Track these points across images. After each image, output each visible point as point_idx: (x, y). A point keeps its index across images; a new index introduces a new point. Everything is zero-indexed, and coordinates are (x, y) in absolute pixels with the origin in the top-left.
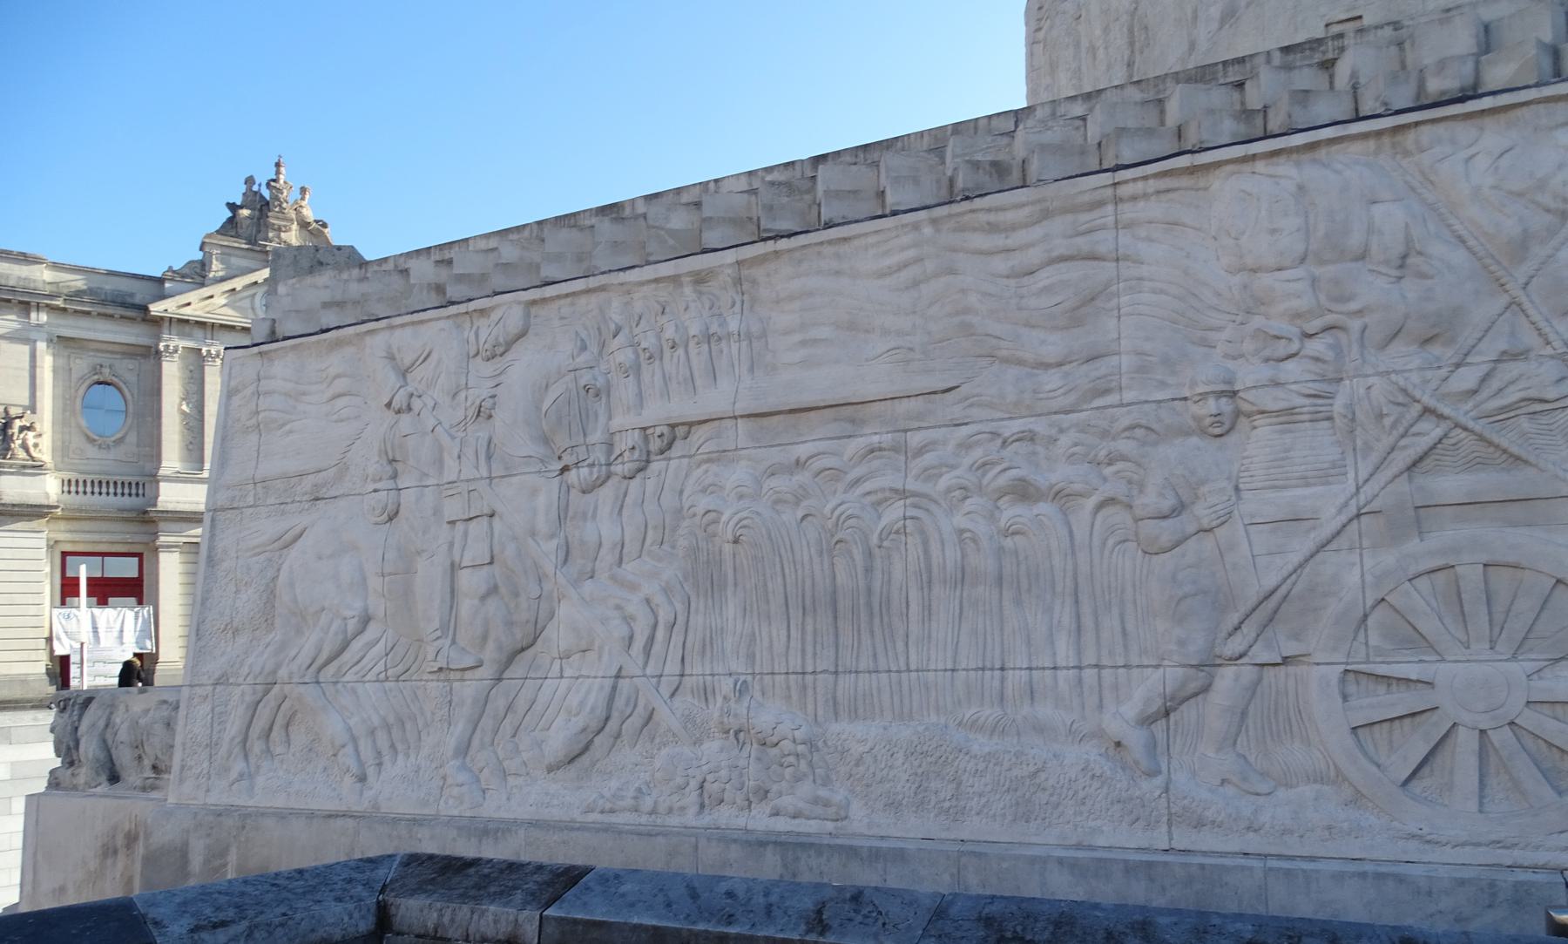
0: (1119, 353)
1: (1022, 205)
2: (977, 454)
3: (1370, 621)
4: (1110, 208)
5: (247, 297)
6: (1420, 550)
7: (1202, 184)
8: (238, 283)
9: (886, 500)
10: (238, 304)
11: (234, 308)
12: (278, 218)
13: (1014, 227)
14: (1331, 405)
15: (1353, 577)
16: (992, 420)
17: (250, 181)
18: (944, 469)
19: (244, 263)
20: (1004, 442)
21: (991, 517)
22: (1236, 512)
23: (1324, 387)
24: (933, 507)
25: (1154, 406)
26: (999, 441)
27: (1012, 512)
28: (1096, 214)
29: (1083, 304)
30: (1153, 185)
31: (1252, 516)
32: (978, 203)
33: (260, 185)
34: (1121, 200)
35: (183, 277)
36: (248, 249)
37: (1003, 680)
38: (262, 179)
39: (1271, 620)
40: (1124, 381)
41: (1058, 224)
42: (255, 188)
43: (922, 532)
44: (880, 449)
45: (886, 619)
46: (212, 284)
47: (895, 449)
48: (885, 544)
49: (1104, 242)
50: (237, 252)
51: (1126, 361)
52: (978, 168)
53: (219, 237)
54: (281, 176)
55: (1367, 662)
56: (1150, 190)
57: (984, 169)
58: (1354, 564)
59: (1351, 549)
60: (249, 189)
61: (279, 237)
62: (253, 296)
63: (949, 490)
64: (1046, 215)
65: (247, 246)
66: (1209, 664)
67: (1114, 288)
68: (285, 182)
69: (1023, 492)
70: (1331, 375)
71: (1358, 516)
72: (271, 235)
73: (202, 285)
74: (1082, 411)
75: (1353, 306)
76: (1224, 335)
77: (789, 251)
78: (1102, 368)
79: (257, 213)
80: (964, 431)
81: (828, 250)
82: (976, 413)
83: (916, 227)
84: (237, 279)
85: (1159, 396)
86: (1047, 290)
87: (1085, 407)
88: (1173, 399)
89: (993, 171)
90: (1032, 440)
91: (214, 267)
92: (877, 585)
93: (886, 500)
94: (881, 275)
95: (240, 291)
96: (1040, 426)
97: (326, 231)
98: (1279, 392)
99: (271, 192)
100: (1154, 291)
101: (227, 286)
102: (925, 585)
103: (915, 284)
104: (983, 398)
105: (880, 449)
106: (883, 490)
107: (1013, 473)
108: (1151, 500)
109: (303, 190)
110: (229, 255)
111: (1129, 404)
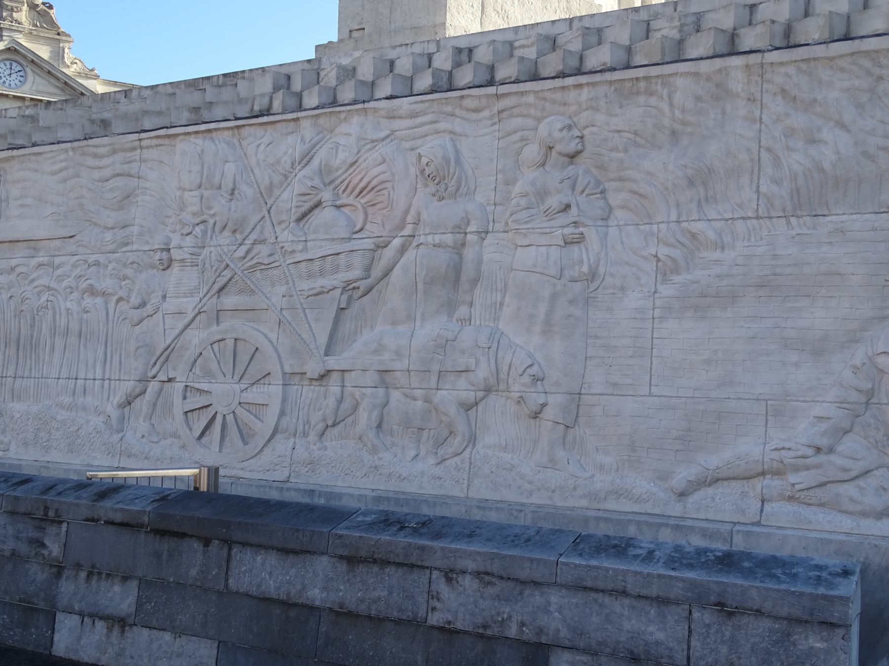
0: (134, 225)
1: (104, 146)
2: (78, 271)
3: (197, 363)
4: (139, 151)
6: (215, 331)
7: (173, 143)
9: (43, 291)
13: (102, 157)
14: (198, 259)
15: (196, 341)
16: (86, 254)
18: (65, 277)
20: (89, 265)
21: (79, 303)
22: (161, 307)
23: (197, 250)
24: (59, 297)
25: (142, 253)
26: (87, 265)
27: (88, 301)
28: (133, 153)
29: (124, 199)
30: (155, 142)
31: (166, 310)
32: (90, 142)
34: (143, 148)
37: (76, 383)
39: (167, 361)
40: (134, 240)
41: (119, 157)
43: (54, 308)
44: (43, 265)
45: (37, 351)
47: (48, 265)
48: (40, 313)
49: (134, 168)
51: (135, 229)
52: (94, 123)
55: (193, 382)
56: (153, 144)
57: (97, 124)
58: (196, 336)
59: (197, 328)
61: (11, 16)
63: (65, 288)
64: (114, 152)
66: (144, 380)
67: (137, 192)
69: (92, 291)
70: (200, 245)
71: (200, 313)
72: (4, 14)
74: (118, 253)
75: (212, 212)
76: (171, 220)
77: (18, 156)
78: (127, 231)
80: (76, 258)
81: (33, 158)
82: (81, 250)
83: (66, 151)
85: (146, 248)
86: (111, 190)
87: (119, 251)
88: (150, 250)
89: (101, 125)
90: (99, 265)
92: (35, 334)
93: (43, 291)
94: (53, 174)
96: (102, 258)
97: (51, 12)
98: (180, 251)
100: (151, 195)
102: (53, 335)
103: (65, 180)
104: (84, 242)
105: (43, 265)
106: (41, 285)
107: (89, 281)
108: (135, 300)
111: (134, 251)
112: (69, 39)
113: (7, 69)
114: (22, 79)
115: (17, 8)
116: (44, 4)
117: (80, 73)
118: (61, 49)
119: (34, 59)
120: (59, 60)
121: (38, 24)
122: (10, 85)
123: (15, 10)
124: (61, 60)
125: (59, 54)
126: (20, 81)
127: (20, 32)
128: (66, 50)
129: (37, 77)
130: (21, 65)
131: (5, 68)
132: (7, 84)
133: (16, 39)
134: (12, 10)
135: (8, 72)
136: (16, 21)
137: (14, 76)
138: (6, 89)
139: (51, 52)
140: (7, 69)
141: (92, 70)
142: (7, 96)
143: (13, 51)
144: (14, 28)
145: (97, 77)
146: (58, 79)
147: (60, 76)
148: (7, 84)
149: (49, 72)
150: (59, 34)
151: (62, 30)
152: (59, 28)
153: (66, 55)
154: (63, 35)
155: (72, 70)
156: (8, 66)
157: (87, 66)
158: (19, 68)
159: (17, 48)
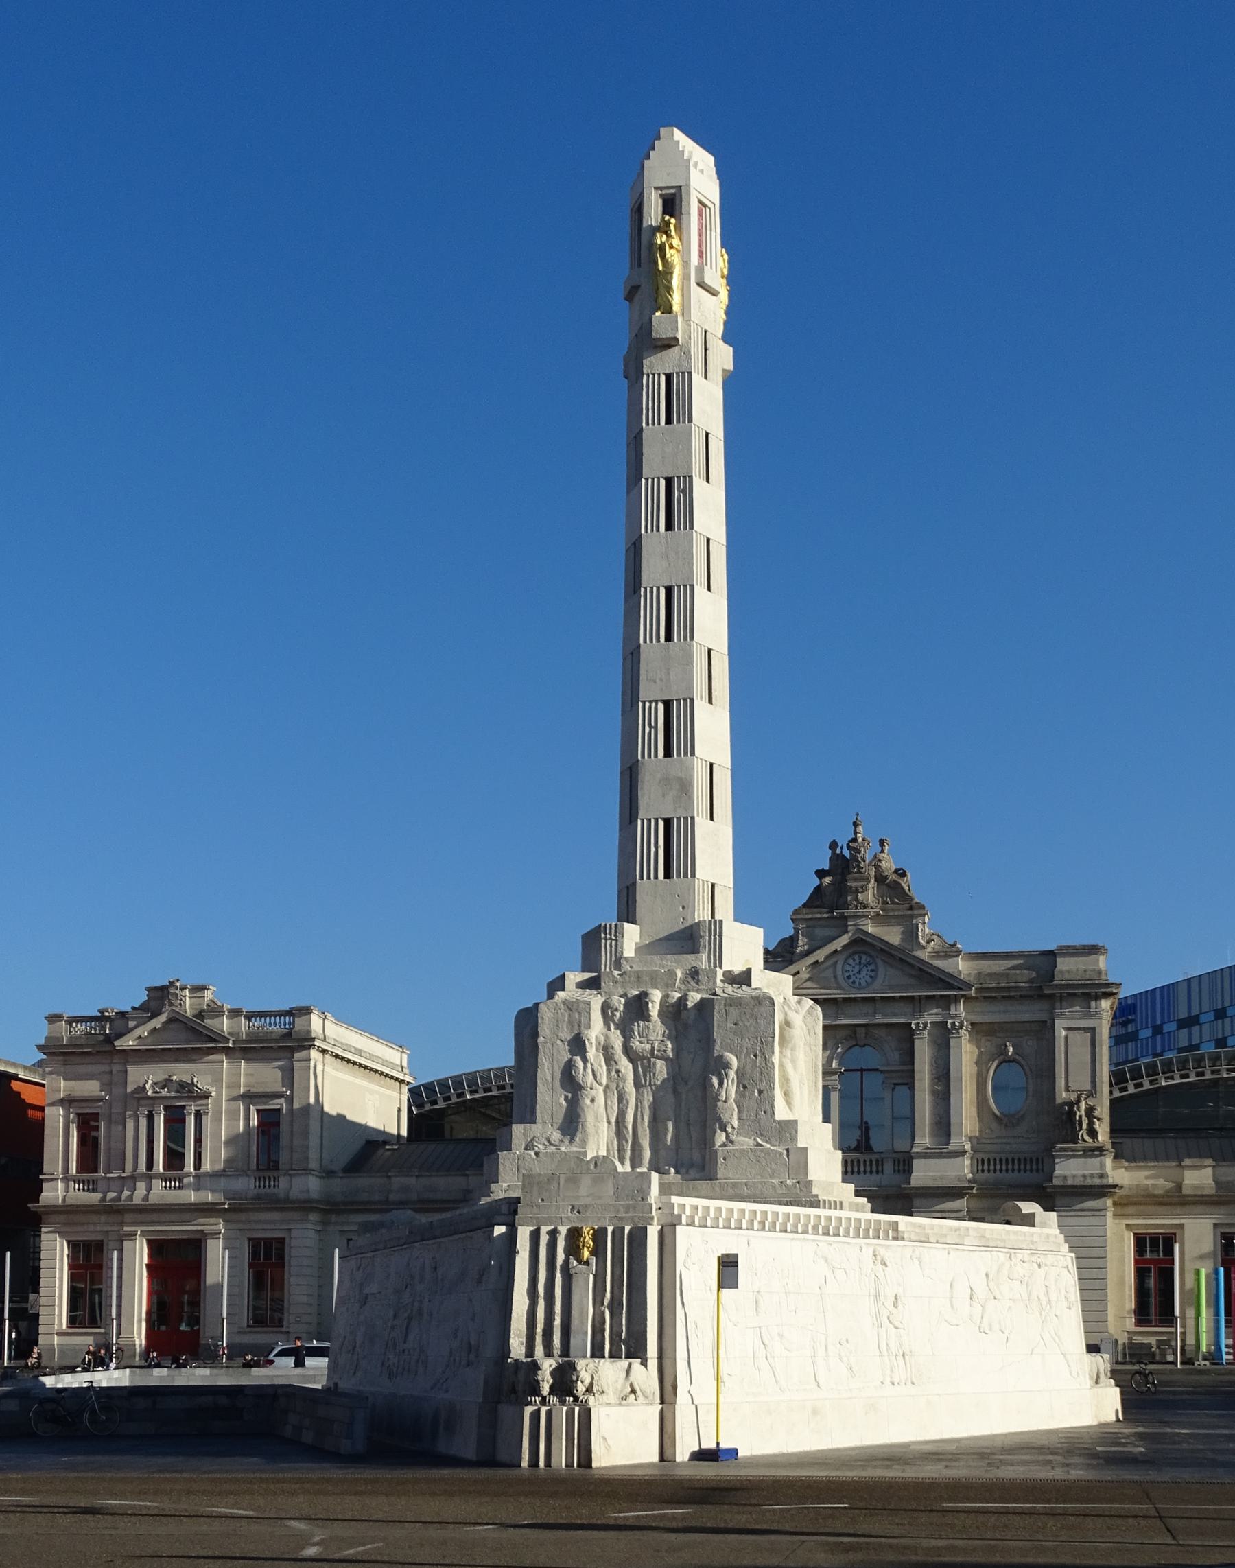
5: (829, 966)
8: (820, 955)
10: (823, 975)
11: (817, 983)
17: (834, 845)
19: (827, 932)
33: (842, 848)
35: (777, 957)
38: (843, 841)
42: (838, 851)
50: (821, 922)
53: (808, 910)
54: (859, 835)
60: (834, 853)
61: (857, 899)
68: (863, 840)
73: (791, 962)
84: (818, 952)
91: (800, 943)
95: (823, 962)
99: (851, 853)
101: (810, 960)
109: (882, 843)
110: (814, 927)
112: (922, 912)
113: (856, 964)
114: (872, 974)
117: (938, 952)
119: (882, 947)
122: (860, 984)
124: (915, 941)
125: (911, 934)
126: (871, 977)
127: (867, 917)
128: (920, 926)
130: (871, 956)
131: (853, 964)
132: (857, 983)
133: (861, 927)
135: (857, 969)
136: (861, 904)
137: (864, 972)
138: (854, 991)
139: (903, 933)
140: (856, 964)
141: (952, 946)
142: (855, 999)
143: (862, 944)
144: (858, 914)
145: (959, 952)
146: (912, 966)
149: (901, 960)
150: (911, 908)
151: (916, 900)
152: (912, 899)
153: (920, 934)
155: (930, 950)
156: (857, 961)
158: (869, 959)
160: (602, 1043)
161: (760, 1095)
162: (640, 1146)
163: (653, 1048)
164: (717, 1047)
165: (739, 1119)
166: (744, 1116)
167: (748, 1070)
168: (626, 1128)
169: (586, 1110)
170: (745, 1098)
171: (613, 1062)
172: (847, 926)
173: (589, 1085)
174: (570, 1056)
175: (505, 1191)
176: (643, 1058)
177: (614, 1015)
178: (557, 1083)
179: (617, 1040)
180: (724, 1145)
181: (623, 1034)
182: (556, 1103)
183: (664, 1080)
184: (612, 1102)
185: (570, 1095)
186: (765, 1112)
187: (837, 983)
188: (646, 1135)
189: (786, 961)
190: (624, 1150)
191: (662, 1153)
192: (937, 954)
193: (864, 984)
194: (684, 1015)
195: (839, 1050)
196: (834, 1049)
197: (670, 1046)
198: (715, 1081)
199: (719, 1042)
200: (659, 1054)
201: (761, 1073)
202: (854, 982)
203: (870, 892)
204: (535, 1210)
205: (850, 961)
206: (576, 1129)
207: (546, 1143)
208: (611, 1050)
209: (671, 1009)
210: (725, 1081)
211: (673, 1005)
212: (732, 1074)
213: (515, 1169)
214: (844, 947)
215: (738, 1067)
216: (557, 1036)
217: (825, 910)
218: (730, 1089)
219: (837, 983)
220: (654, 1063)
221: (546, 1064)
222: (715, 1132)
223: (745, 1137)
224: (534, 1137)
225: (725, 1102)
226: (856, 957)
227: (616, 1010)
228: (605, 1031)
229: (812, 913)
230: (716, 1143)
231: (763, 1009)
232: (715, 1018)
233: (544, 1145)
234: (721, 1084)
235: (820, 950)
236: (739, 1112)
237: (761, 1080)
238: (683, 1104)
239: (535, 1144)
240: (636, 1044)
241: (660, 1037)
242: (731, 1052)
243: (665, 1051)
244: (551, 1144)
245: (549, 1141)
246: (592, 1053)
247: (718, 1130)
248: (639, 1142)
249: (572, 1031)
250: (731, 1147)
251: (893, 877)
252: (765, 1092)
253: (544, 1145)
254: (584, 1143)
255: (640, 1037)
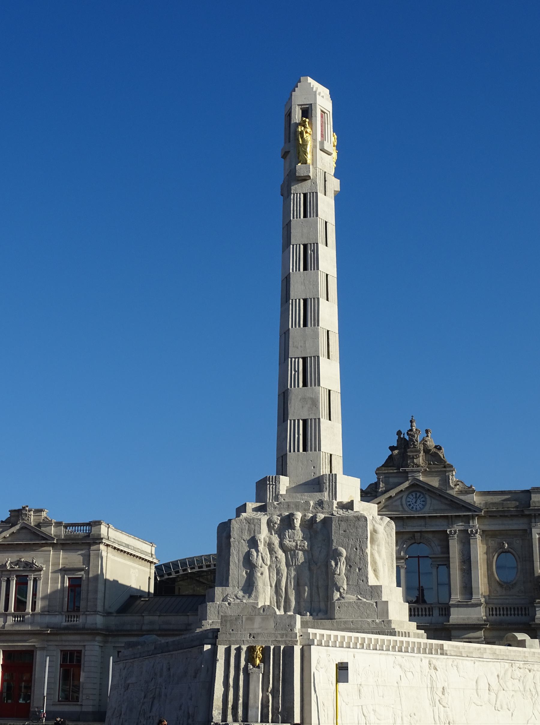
8: (393, 493)
10: (394, 504)
12: (412, 452)
19: (396, 480)
36: (397, 472)
46: (380, 495)
53: (386, 468)
61: (413, 462)
62: (402, 498)
65: (397, 471)
72: (409, 462)
73: (376, 497)
79: (403, 450)
84: (391, 491)
91: (381, 486)
95: (394, 496)
101: (387, 495)
110: (389, 477)
113: (414, 498)
115: (416, 455)
116: (436, 447)
117: (461, 491)
118: (447, 477)
119: (428, 488)
120: (446, 485)
121: (432, 462)
122: (416, 509)
123: (415, 457)
125: (445, 481)
126: (423, 505)
127: (419, 472)
129: (433, 500)
130: (423, 494)
131: (412, 498)
132: (414, 509)
134: (413, 458)
135: (414, 500)
136: (416, 465)
137: (419, 501)
138: (413, 512)
139: (440, 481)
140: (414, 498)
142: (414, 517)
143: (417, 487)
144: (414, 470)
145: (473, 491)
146: (446, 499)
147: (447, 497)
148: (414, 509)
149: (440, 495)
150: (445, 467)
151: (448, 463)
152: (445, 462)
153: (450, 481)
154: (448, 467)
155: (456, 490)
156: (414, 496)
157: (466, 485)
159: (418, 483)
160: (268, 542)
161: (359, 571)
162: (289, 599)
163: (297, 545)
164: (334, 544)
165: (348, 584)
166: (350, 583)
167: (352, 557)
168: (281, 589)
169: (258, 579)
170: (350, 572)
171: (273, 552)
172: (408, 477)
173: (260, 565)
174: (248, 549)
175: (211, 625)
176: (291, 550)
177: (274, 526)
178: (241, 564)
179: (276, 540)
180: (339, 599)
181: (280, 537)
182: (240, 575)
183: (302, 563)
184: (273, 575)
185: (248, 571)
186: (362, 581)
187: (403, 508)
188: (293, 594)
189: (372, 496)
190: (280, 602)
191: (303, 604)
192: (461, 492)
193: (418, 508)
194: (315, 526)
195: (405, 546)
196: (402, 545)
197: (306, 543)
198: (333, 563)
199: (335, 541)
200: (300, 548)
201: (360, 559)
202: (413, 508)
203: (421, 458)
204: (228, 636)
205: (410, 496)
206: (252, 590)
207: (235, 598)
208: (273, 546)
209: (307, 523)
210: (339, 563)
211: (308, 521)
212: (343, 559)
213: (216, 613)
214: (407, 488)
215: (346, 555)
216: (242, 538)
217: (395, 468)
218: (342, 568)
219: (403, 508)
220: (298, 553)
221: (235, 553)
222: (334, 592)
223: (351, 595)
224: (228, 594)
225: (339, 575)
226: (414, 494)
227: (276, 523)
228: (269, 535)
229: (388, 470)
230: (334, 598)
231: (361, 523)
232: (333, 528)
233: (234, 598)
234: (336, 565)
235: (393, 490)
236: (347, 581)
237: (360, 563)
238: (315, 576)
239: (228, 598)
240: (287, 542)
241: (301, 539)
242: (342, 547)
243: (304, 546)
244: (237, 598)
245: (236, 597)
246: (261, 547)
247: (335, 591)
248: (289, 598)
249: (250, 534)
250: (343, 601)
251: (434, 450)
252: (362, 569)
253: (234, 598)
254: (257, 598)
255: (289, 538)
